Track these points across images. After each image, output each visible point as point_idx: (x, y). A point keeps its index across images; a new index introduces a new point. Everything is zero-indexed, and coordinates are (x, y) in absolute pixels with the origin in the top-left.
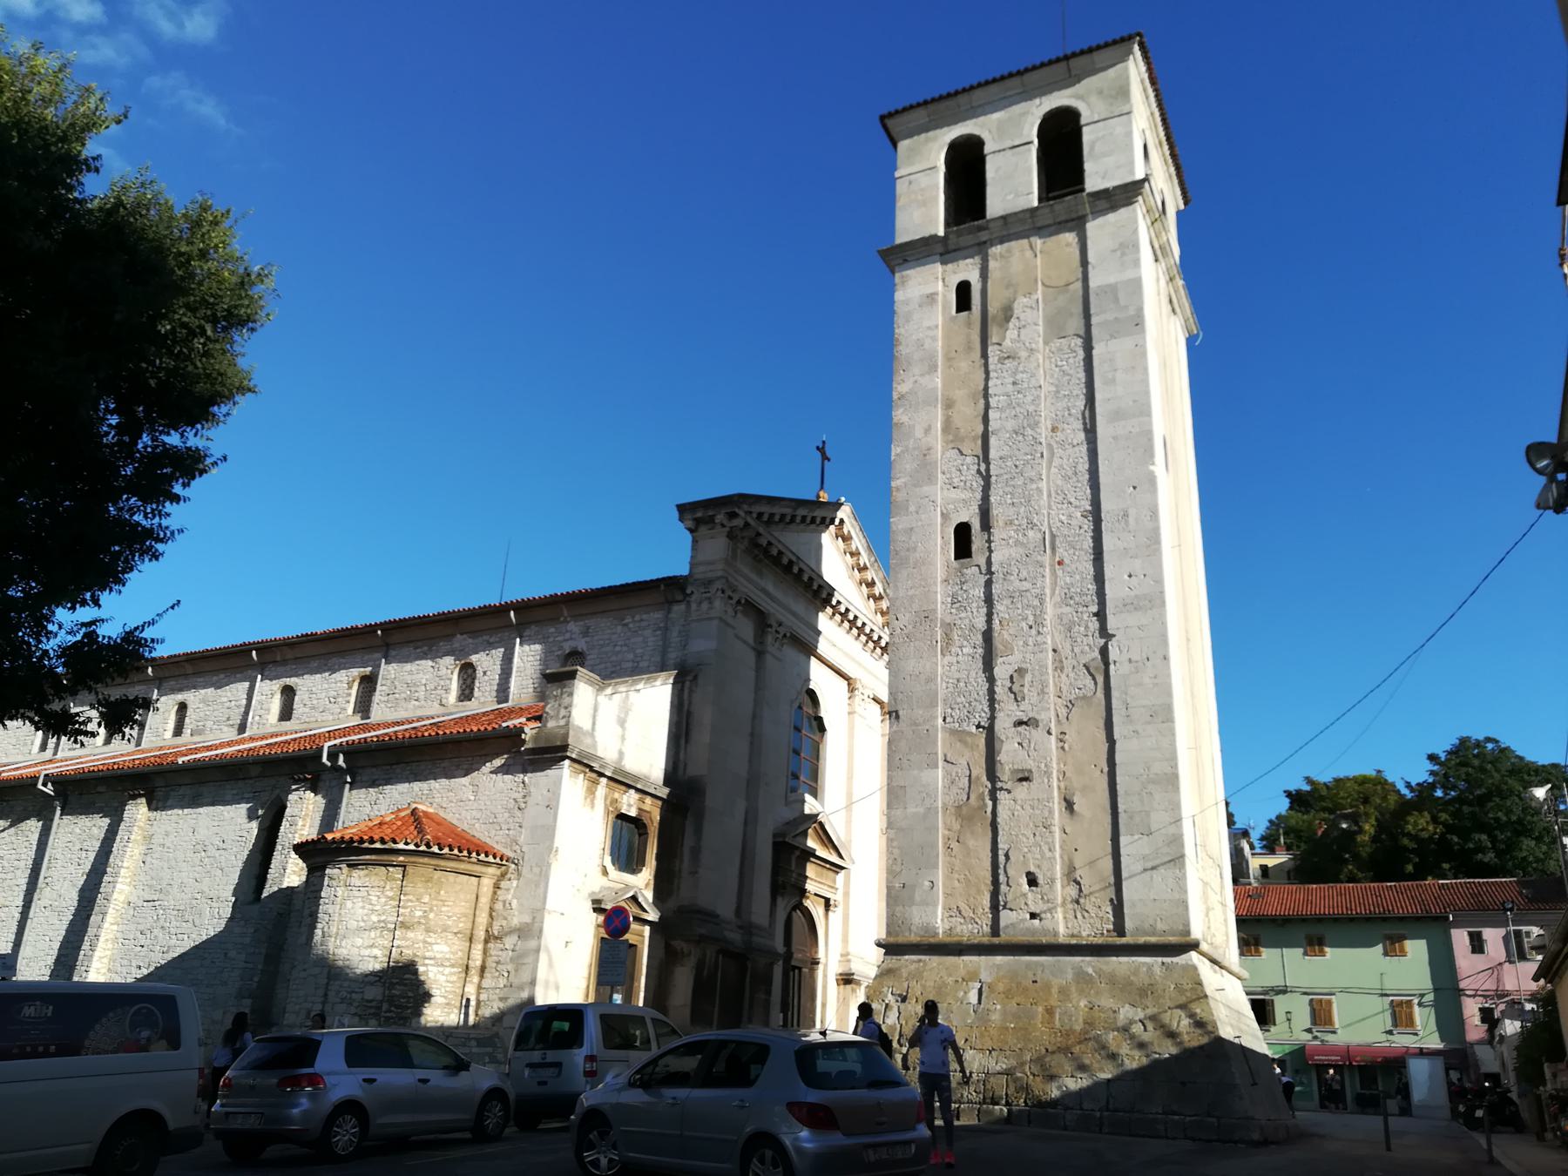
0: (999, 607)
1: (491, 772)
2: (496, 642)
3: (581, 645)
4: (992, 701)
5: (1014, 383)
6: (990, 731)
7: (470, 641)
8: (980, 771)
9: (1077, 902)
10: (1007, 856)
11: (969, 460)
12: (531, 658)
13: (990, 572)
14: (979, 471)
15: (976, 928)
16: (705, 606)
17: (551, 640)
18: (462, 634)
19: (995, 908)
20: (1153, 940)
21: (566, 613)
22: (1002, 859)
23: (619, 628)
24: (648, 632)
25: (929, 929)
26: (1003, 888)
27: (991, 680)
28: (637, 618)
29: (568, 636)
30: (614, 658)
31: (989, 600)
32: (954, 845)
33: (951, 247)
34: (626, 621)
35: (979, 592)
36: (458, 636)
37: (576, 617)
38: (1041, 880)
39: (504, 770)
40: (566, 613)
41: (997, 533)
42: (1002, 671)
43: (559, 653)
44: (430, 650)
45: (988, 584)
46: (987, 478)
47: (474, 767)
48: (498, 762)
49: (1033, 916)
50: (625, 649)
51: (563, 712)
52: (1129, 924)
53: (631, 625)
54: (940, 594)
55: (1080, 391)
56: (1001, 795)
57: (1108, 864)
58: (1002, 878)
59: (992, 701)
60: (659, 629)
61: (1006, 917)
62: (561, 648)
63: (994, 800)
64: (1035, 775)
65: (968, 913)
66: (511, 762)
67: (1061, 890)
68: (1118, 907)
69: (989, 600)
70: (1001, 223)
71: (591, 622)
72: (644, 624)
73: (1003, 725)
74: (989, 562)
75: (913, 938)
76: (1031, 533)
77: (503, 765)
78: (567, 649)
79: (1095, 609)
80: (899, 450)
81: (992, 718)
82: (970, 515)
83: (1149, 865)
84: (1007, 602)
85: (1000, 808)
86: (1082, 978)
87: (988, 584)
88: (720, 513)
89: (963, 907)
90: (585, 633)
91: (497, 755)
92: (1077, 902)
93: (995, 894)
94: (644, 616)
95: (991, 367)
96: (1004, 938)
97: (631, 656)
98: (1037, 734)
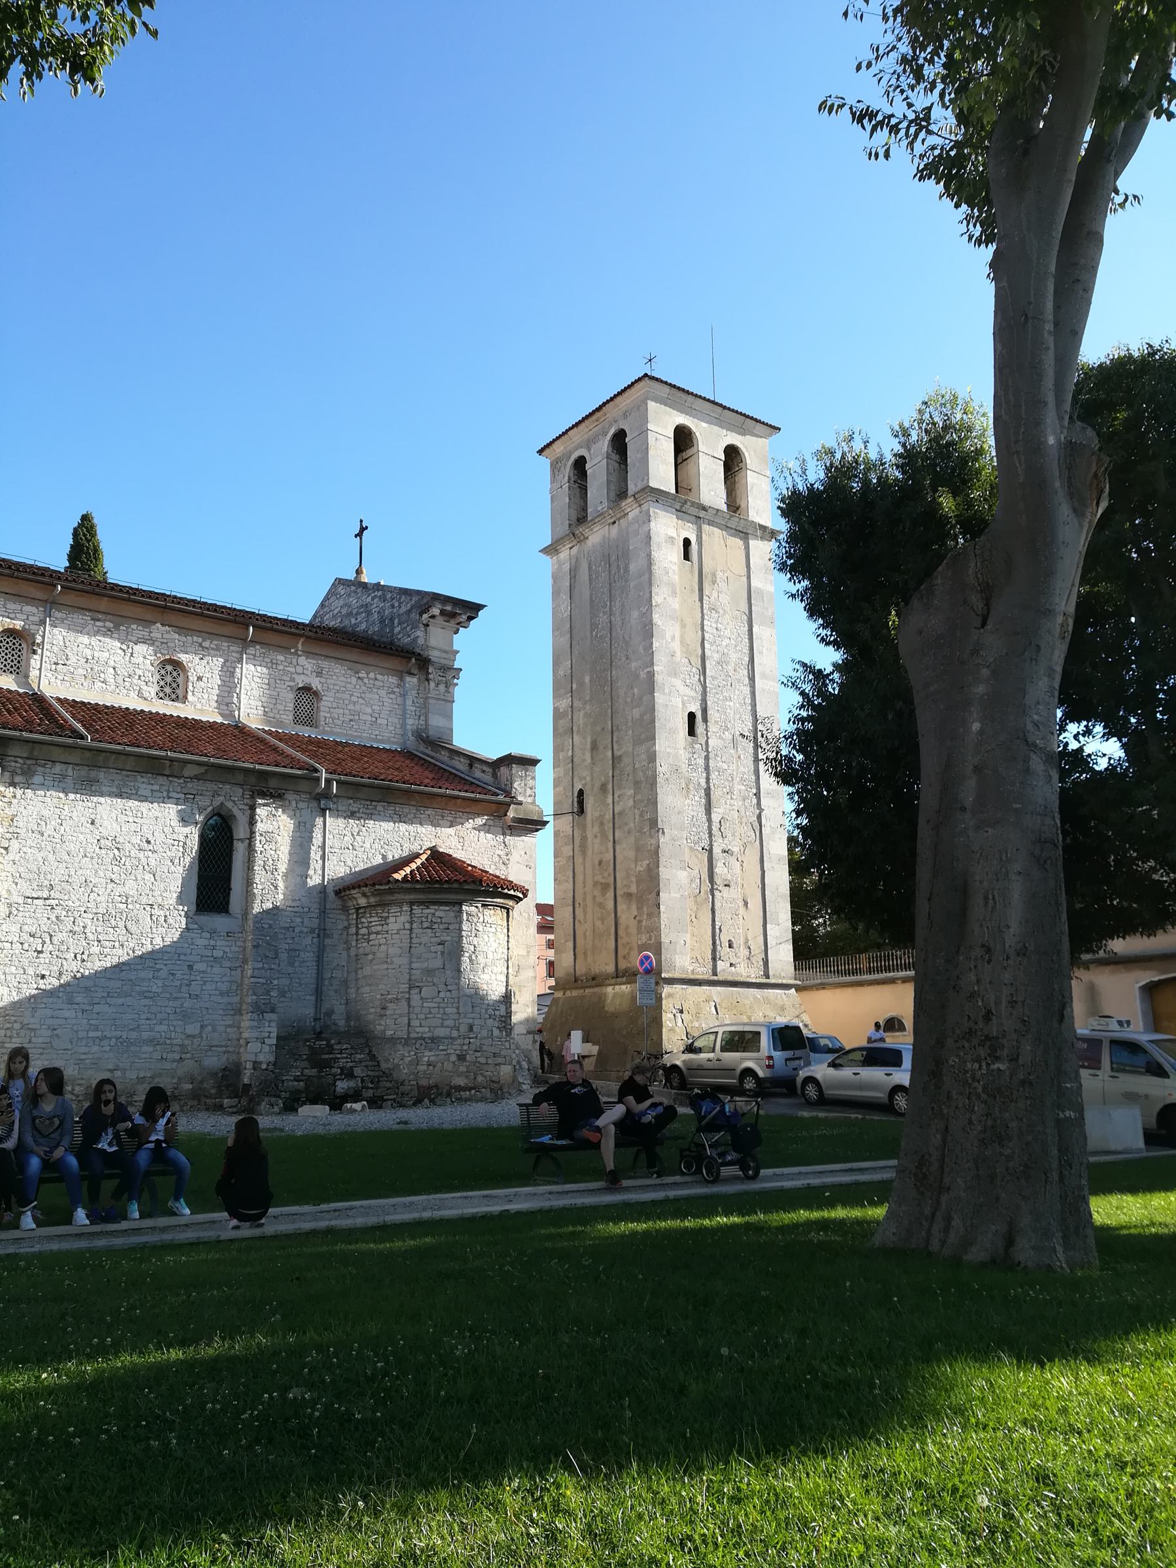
0: (713, 776)
1: (474, 829)
2: (213, 649)
3: (316, 683)
4: (710, 835)
5: (717, 629)
6: (710, 851)
7: (177, 636)
8: (705, 876)
9: (749, 959)
10: (720, 929)
11: (694, 670)
12: (258, 680)
13: (707, 751)
14: (699, 679)
15: (704, 972)
16: (442, 688)
17: (281, 667)
18: (163, 625)
19: (714, 959)
20: (780, 981)
21: (300, 646)
22: (718, 931)
23: (354, 680)
24: (383, 693)
25: (684, 970)
26: (719, 947)
27: (709, 820)
28: (372, 675)
29: (299, 669)
30: (351, 707)
31: (707, 768)
32: (694, 919)
33: (684, 509)
34: (360, 675)
35: (701, 762)
36: (158, 625)
37: (308, 654)
38: (735, 946)
39: (486, 828)
40: (300, 646)
41: (713, 728)
42: (715, 818)
43: (292, 684)
44: (117, 627)
45: (707, 758)
46: (704, 687)
47: (458, 820)
48: (480, 821)
49: (731, 965)
50: (361, 701)
51: (529, 792)
52: (771, 973)
53: (366, 681)
54: (684, 755)
55: (746, 650)
56: (716, 893)
57: (761, 938)
58: (718, 942)
59: (710, 835)
60: (394, 693)
61: (721, 965)
62: (293, 680)
63: (713, 895)
64: (732, 884)
65: (701, 961)
66: (491, 823)
67: (744, 952)
68: (766, 962)
69: (707, 768)
70: (715, 512)
71: (325, 664)
72: (377, 683)
73: (717, 850)
74: (707, 742)
75: (677, 975)
76: (726, 733)
77: (485, 824)
78: (301, 681)
79: (754, 791)
80: (658, 644)
81: (711, 845)
82: (695, 708)
83: (779, 942)
84: (717, 773)
85: (716, 900)
86: (767, 1000)
87: (707, 758)
88: (465, 614)
89: (699, 957)
90: (319, 674)
91: (479, 815)
92: (749, 959)
93: (714, 951)
94: (379, 677)
95: (705, 611)
96: (720, 977)
97: (369, 710)
98: (732, 860)
